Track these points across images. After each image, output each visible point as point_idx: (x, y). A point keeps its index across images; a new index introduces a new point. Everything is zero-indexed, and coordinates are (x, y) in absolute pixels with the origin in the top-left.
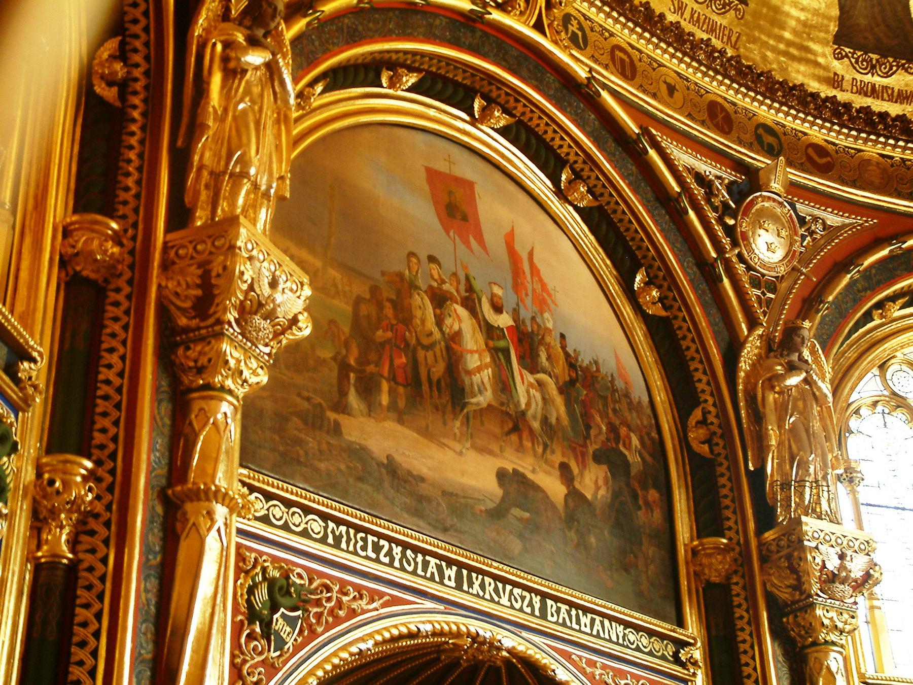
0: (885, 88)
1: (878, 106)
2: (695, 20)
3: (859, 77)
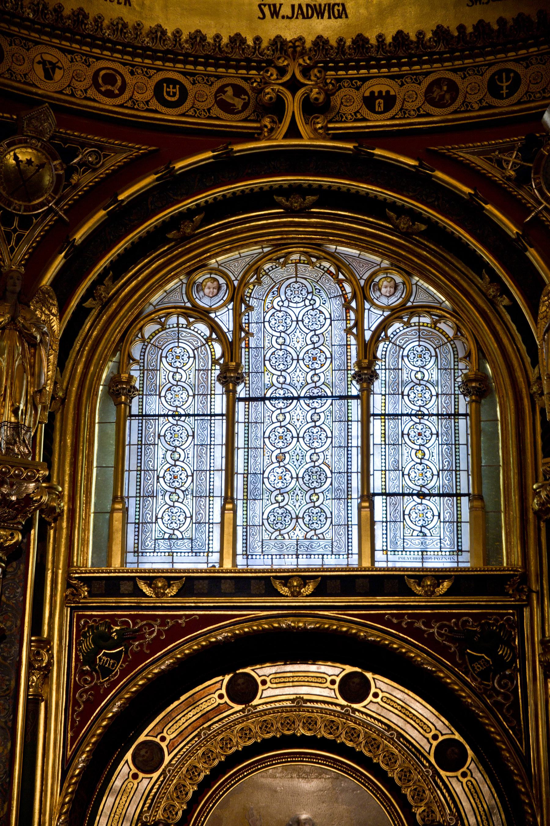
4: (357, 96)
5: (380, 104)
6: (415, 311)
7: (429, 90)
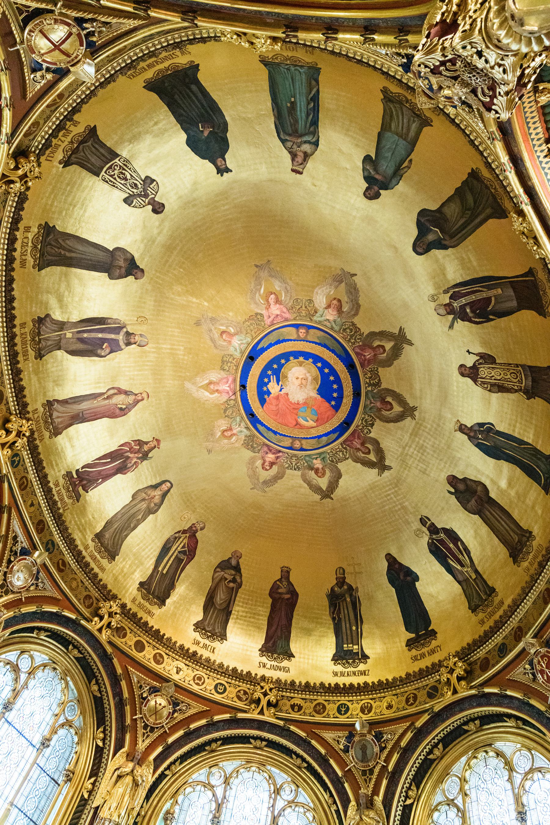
0: (99, 561)
1: (93, 565)
2: (59, 492)
3: (94, 551)
4: (289, 704)
5: (296, 708)
6: (297, 804)
7: (315, 706)
